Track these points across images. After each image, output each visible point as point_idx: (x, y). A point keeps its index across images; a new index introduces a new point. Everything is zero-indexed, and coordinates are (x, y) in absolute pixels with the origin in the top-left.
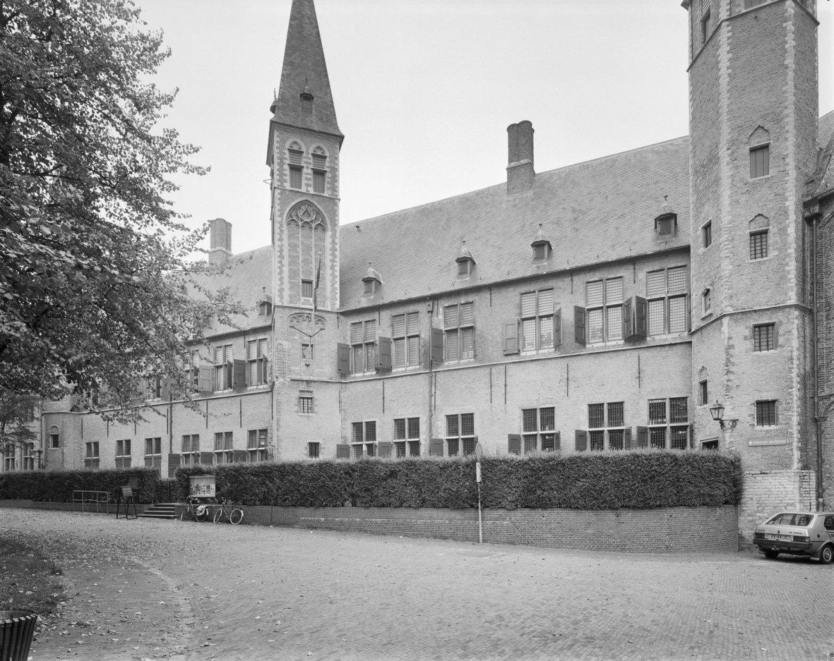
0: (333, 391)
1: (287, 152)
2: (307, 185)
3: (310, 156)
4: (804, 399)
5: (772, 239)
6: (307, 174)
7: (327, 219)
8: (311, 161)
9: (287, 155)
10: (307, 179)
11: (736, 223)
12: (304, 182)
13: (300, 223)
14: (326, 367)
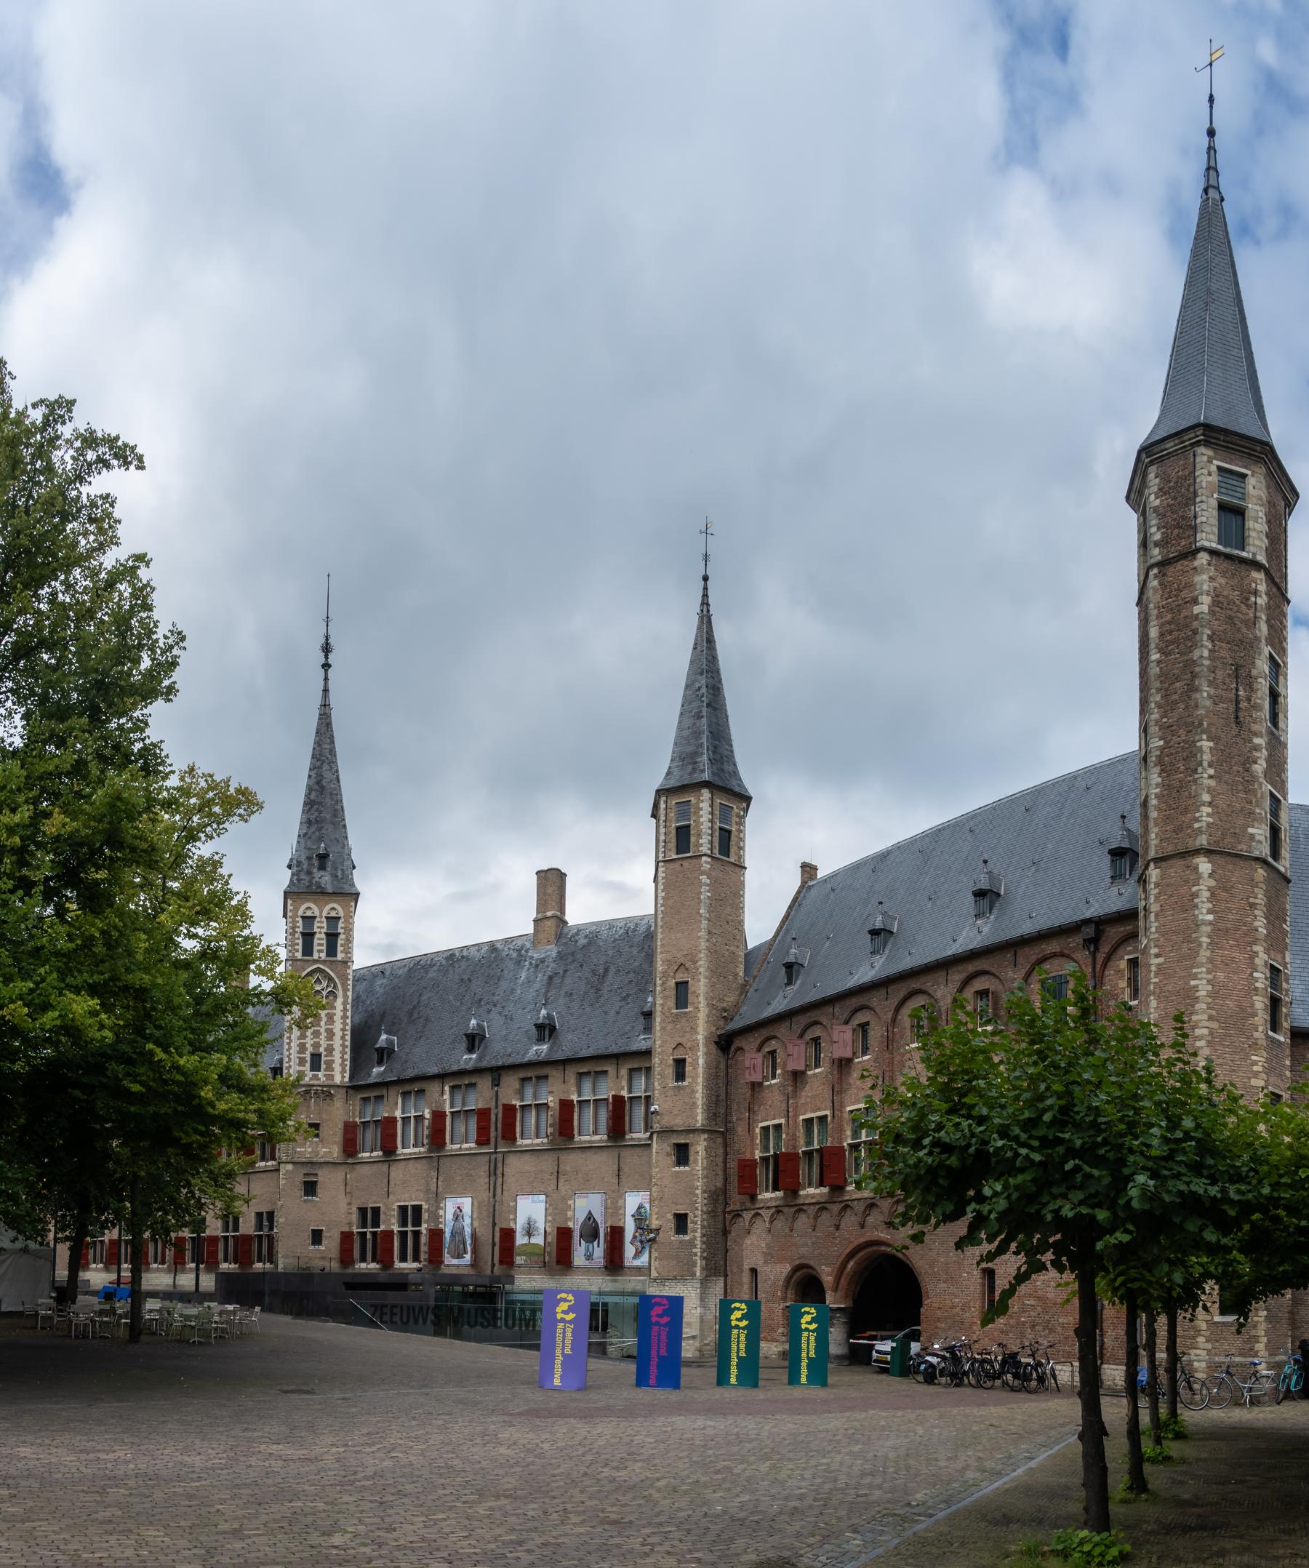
0: (339, 1174)
2: (320, 951)
8: (325, 925)
12: (316, 948)
14: (331, 1149)
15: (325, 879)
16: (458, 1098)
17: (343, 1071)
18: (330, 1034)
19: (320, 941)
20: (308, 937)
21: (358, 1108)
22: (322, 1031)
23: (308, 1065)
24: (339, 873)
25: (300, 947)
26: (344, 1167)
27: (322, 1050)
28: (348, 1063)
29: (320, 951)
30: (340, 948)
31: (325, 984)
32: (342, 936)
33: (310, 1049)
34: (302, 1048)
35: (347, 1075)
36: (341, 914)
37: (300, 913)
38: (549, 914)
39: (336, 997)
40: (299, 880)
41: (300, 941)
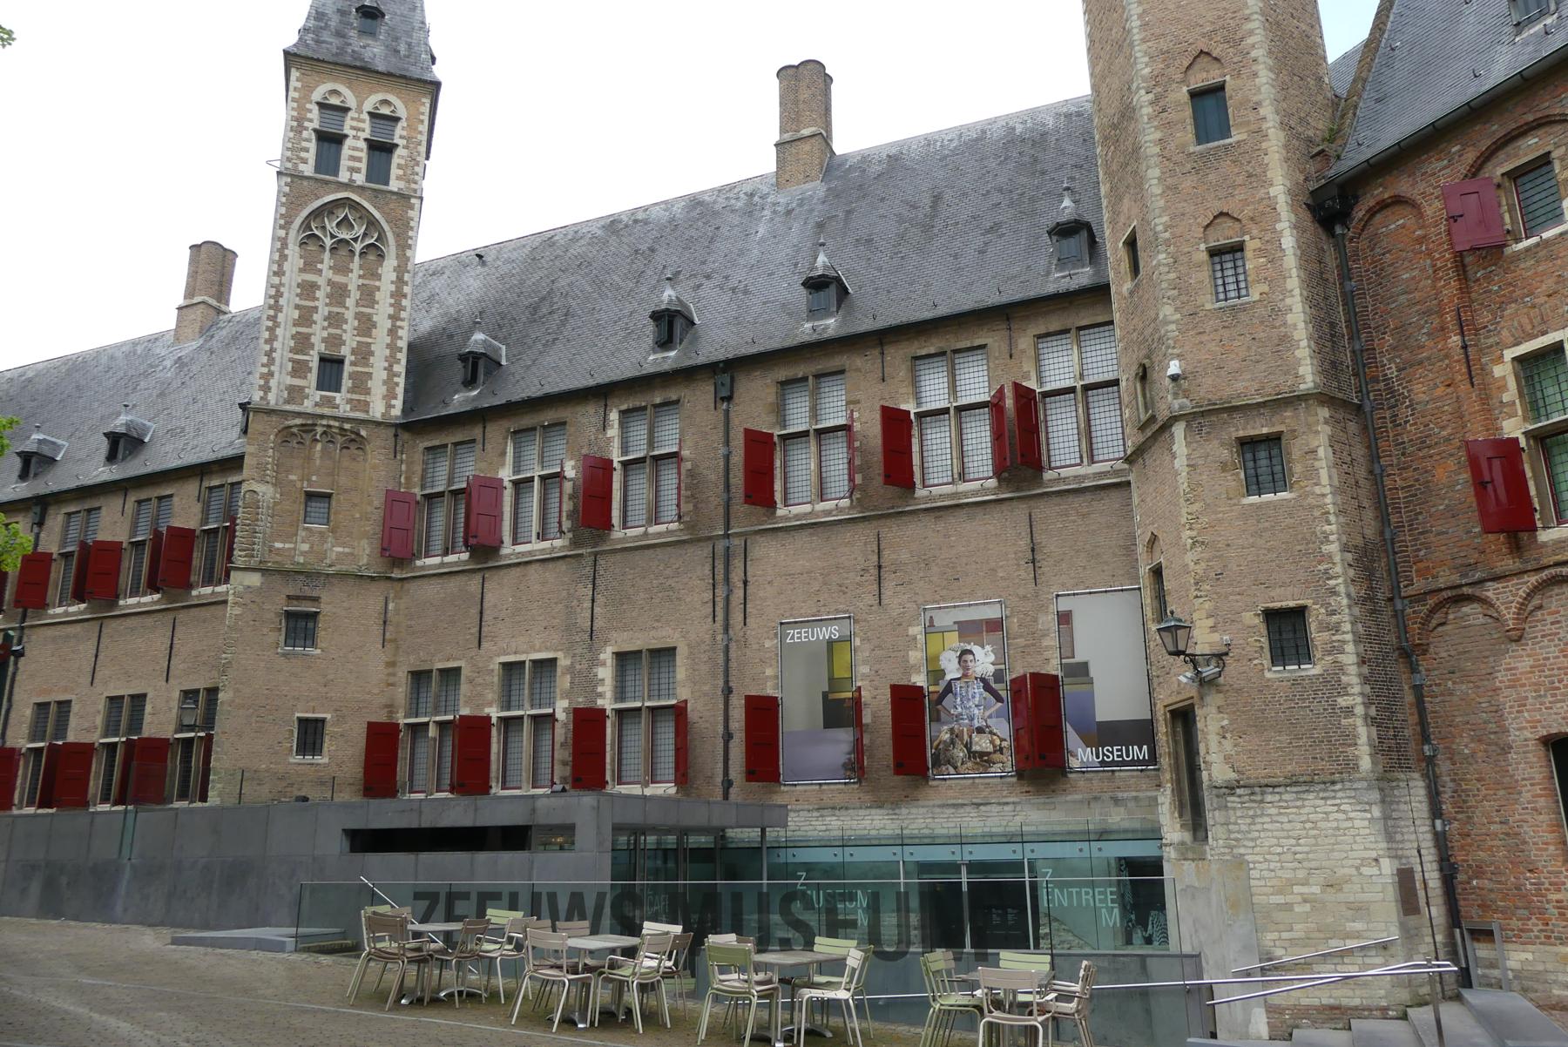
0: (371, 600)
1: (316, 109)
2: (352, 170)
3: (367, 117)
4: (1367, 601)
5: (1252, 262)
6: (355, 149)
7: (390, 235)
8: (367, 125)
9: (315, 112)
10: (352, 158)
11: (1178, 231)
13: (328, 242)
15: (374, 51)
16: (639, 432)
17: (390, 395)
18: (366, 325)
19: (354, 151)
20: (330, 140)
21: (418, 468)
22: (349, 315)
23: (313, 377)
24: (403, 48)
25: (311, 156)
26: (383, 585)
27: (345, 351)
28: (401, 381)
29: (352, 170)
30: (394, 172)
31: (359, 230)
32: (399, 152)
33: (319, 347)
34: (302, 343)
35: (398, 403)
36: (402, 112)
37: (317, 95)
38: (806, 132)
39: (381, 256)
40: (317, 42)
41: (312, 146)
